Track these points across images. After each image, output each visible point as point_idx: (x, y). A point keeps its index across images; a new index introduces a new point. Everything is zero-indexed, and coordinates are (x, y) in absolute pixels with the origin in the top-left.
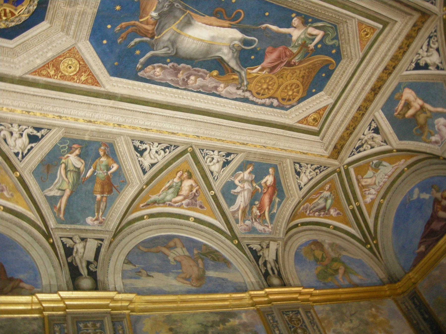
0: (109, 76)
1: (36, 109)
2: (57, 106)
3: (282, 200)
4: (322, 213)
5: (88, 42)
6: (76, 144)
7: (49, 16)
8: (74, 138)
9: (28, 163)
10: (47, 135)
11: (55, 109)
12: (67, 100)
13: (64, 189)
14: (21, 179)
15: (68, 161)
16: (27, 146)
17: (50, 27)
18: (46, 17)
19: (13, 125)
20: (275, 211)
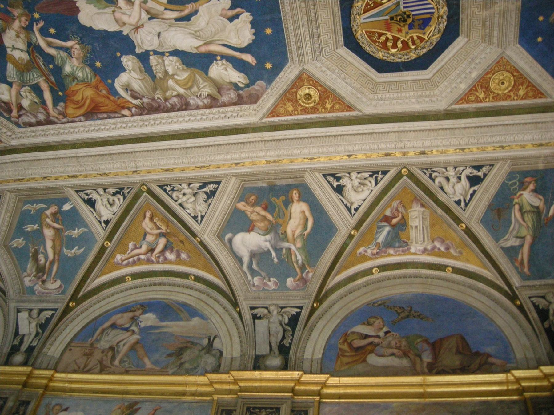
2: (495, 135)
5: (518, 45)
7: (463, 28)
8: (525, 169)
9: (474, 211)
11: (494, 139)
12: (507, 125)
13: (523, 235)
14: (468, 231)
15: (522, 200)
16: (469, 190)
17: (467, 42)
18: (460, 31)
19: (448, 169)
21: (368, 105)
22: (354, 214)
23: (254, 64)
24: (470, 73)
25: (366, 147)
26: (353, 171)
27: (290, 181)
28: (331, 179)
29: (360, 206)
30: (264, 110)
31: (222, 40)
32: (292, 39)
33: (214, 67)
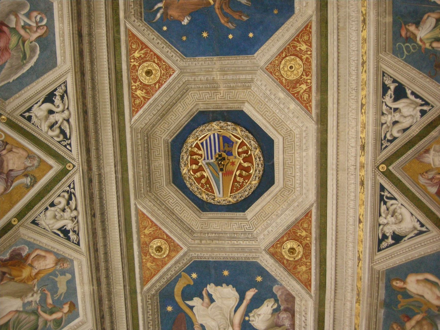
0: (295, 15)
1: (357, 96)
2: (349, 71)
5: (255, 55)
6: (400, 32)
8: (391, 37)
10: (392, 76)
11: (354, 73)
12: (338, 60)
15: (428, 39)
17: (248, 102)
19: (383, 122)
21: (306, 197)
22: (427, 228)
23: (257, 291)
24: (279, 99)
25: (352, 204)
26: (378, 221)
27: (382, 285)
28: (384, 244)
29: (418, 221)
30: (303, 292)
31: (230, 312)
32: (236, 255)
33: (255, 324)
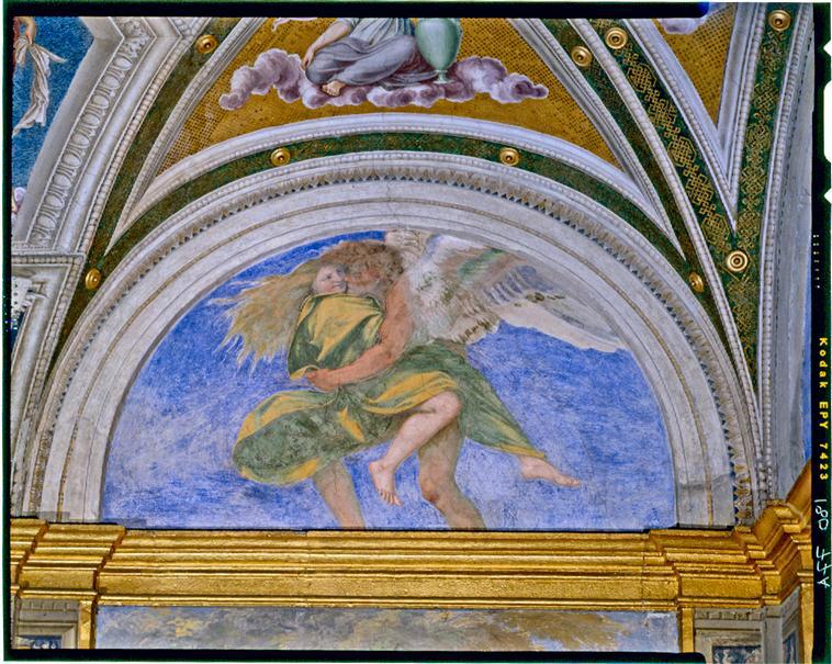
3: (75, 62)
4: (419, 89)
20: (40, 117)
